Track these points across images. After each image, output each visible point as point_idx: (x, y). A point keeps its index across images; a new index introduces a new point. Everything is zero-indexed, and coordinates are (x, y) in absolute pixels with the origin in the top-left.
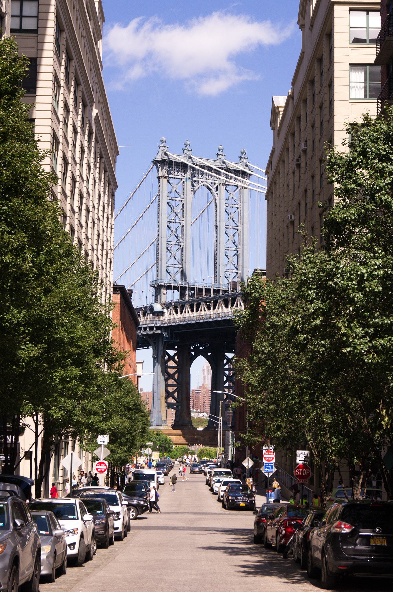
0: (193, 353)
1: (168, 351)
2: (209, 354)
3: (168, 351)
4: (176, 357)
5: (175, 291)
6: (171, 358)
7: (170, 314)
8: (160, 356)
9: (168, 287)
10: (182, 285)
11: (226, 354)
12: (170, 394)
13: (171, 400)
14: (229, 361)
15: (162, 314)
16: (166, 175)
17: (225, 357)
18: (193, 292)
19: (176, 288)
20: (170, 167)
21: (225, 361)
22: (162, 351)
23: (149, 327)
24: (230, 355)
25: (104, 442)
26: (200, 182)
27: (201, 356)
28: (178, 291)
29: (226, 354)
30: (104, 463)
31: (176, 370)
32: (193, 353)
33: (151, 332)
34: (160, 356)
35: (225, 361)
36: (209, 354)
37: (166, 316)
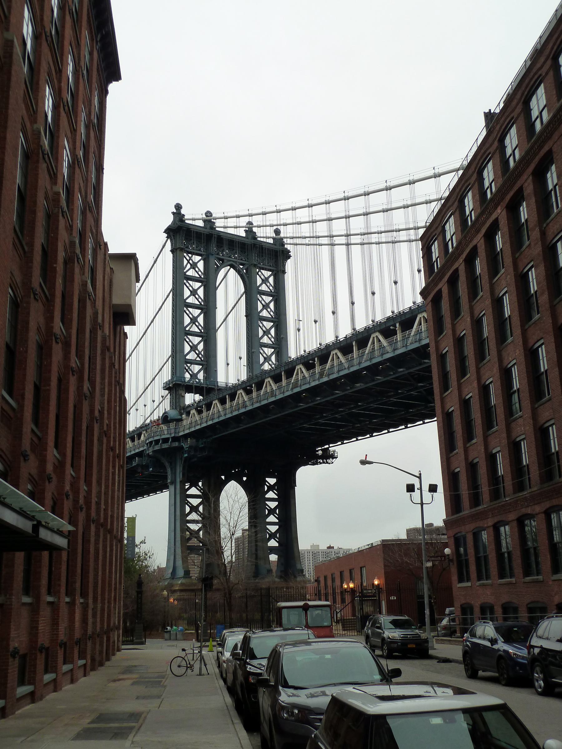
0: (223, 477)
2: (245, 479)
4: (200, 484)
8: (178, 480)
9: (190, 389)
13: (194, 542)
14: (271, 488)
24: (272, 481)
26: (225, 261)
27: (233, 481)
29: (267, 479)
31: (200, 500)
32: (223, 477)
33: (165, 446)
34: (178, 480)
36: (245, 479)
37: (186, 422)
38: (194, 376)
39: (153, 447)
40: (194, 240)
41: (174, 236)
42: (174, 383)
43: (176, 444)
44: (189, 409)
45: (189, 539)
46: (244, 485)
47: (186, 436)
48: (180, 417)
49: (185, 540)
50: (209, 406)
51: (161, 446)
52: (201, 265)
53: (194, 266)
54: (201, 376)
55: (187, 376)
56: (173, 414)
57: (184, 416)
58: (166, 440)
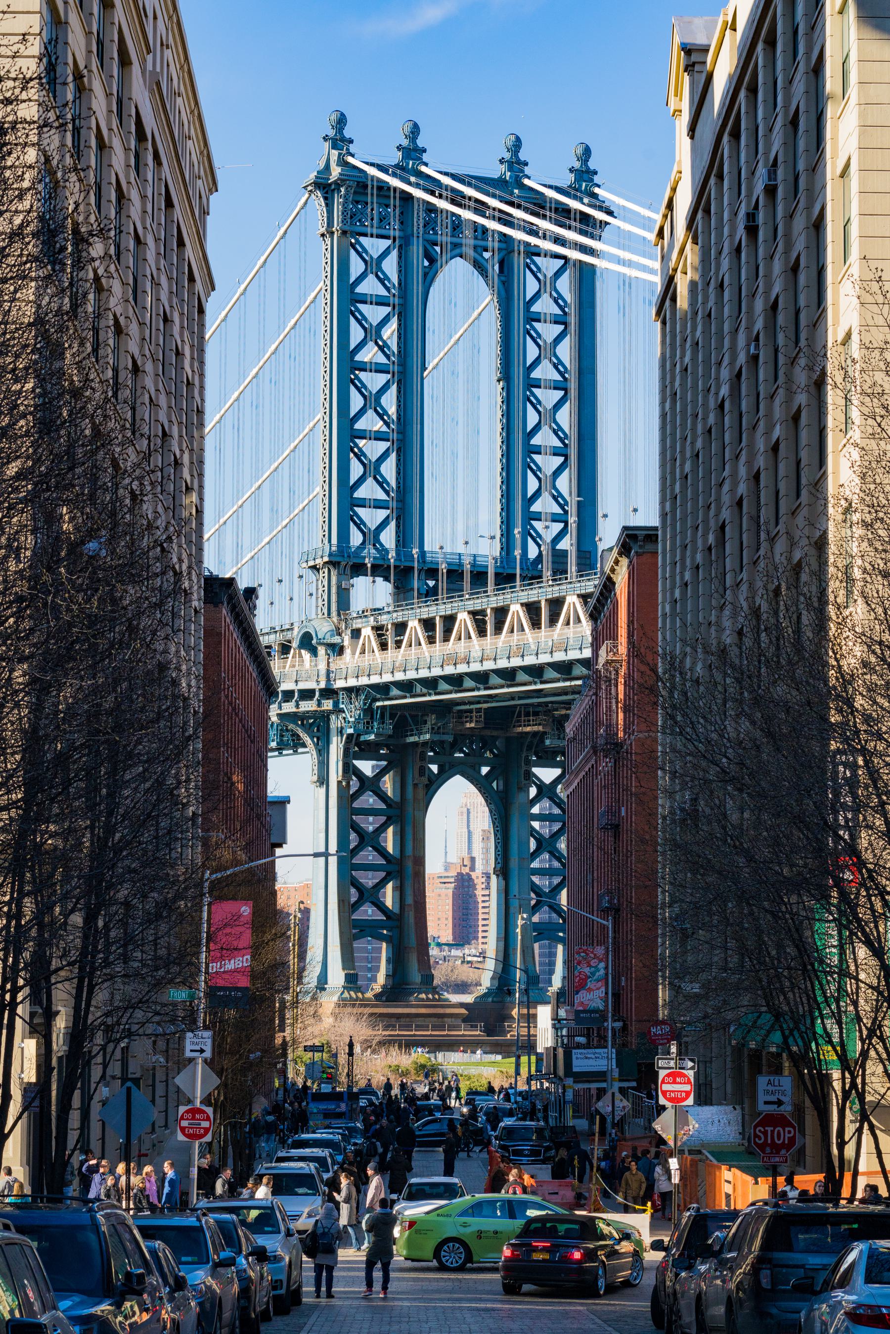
0: (434, 768)
1: (358, 763)
3: (358, 763)
5: (379, 580)
6: (369, 784)
7: (363, 652)
9: (358, 569)
10: (398, 563)
11: (536, 770)
12: (366, 894)
13: (368, 912)
14: (546, 791)
15: (338, 650)
16: (346, 228)
17: (529, 777)
18: (431, 583)
19: (380, 570)
20: (357, 202)
21: (533, 791)
22: (340, 764)
23: (300, 691)
24: (547, 774)
25: (202, 1051)
28: (387, 579)
29: (536, 770)
30: (204, 1112)
32: (434, 768)
35: (533, 791)
38: (372, 537)
39: (280, 708)
40: (372, 203)
41: (326, 199)
42: (326, 559)
43: (328, 705)
44: (357, 624)
45: (355, 906)
46: (482, 784)
47: (349, 690)
48: (336, 640)
49: (347, 908)
50: (400, 628)
51: (297, 706)
52: (390, 266)
53: (373, 266)
54: (388, 538)
55: (356, 538)
56: (322, 628)
57: (347, 640)
58: (307, 695)
